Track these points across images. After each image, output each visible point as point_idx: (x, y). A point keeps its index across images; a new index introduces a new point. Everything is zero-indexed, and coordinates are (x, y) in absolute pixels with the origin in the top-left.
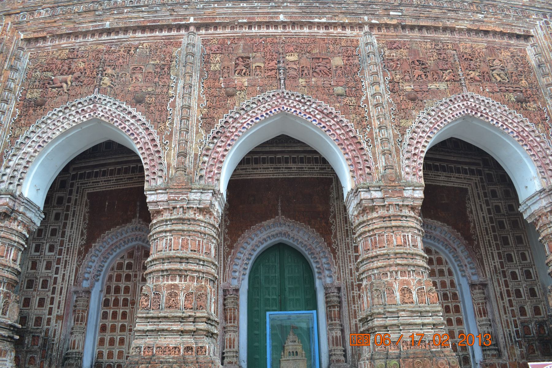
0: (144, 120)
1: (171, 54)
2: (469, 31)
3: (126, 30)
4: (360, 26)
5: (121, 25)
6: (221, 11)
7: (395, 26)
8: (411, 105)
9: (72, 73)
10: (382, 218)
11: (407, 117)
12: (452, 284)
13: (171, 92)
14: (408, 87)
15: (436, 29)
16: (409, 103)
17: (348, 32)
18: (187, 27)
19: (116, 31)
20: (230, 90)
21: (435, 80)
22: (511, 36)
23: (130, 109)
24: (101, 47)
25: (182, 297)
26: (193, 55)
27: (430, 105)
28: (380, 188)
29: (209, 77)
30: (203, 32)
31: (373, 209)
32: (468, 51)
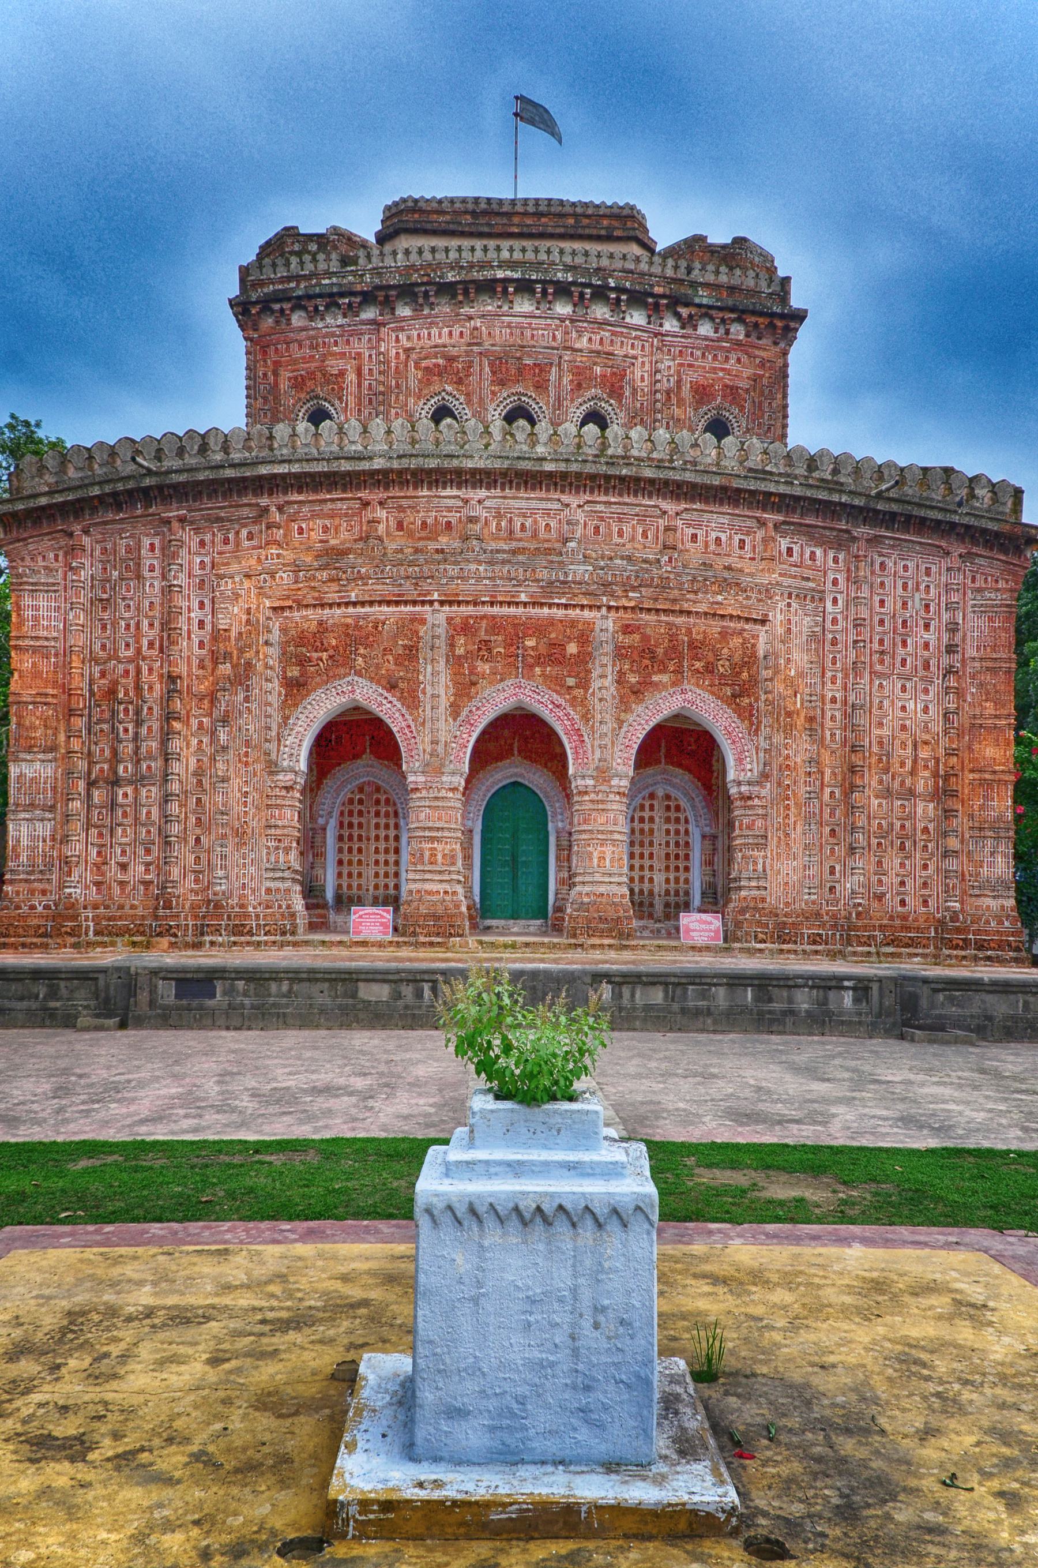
0: (399, 706)
1: (417, 632)
2: (706, 614)
3: (371, 603)
5: (368, 599)
6: (464, 587)
7: (633, 608)
8: (633, 697)
9: (326, 650)
10: (592, 801)
11: (627, 710)
12: (687, 832)
13: (421, 678)
14: (633, 679)
15: (673, 611)
17: (586, 613)
19: (363, 604)
20: (474, 678)
21: (660, 672)
22: (748, 620)
23: (386, 694)
24: (349, 621)
26: (438, 637)
27: (649, 701)
29: (455, 662)
30: (446, 608)
31: (586, 793)
32: (700, 637)
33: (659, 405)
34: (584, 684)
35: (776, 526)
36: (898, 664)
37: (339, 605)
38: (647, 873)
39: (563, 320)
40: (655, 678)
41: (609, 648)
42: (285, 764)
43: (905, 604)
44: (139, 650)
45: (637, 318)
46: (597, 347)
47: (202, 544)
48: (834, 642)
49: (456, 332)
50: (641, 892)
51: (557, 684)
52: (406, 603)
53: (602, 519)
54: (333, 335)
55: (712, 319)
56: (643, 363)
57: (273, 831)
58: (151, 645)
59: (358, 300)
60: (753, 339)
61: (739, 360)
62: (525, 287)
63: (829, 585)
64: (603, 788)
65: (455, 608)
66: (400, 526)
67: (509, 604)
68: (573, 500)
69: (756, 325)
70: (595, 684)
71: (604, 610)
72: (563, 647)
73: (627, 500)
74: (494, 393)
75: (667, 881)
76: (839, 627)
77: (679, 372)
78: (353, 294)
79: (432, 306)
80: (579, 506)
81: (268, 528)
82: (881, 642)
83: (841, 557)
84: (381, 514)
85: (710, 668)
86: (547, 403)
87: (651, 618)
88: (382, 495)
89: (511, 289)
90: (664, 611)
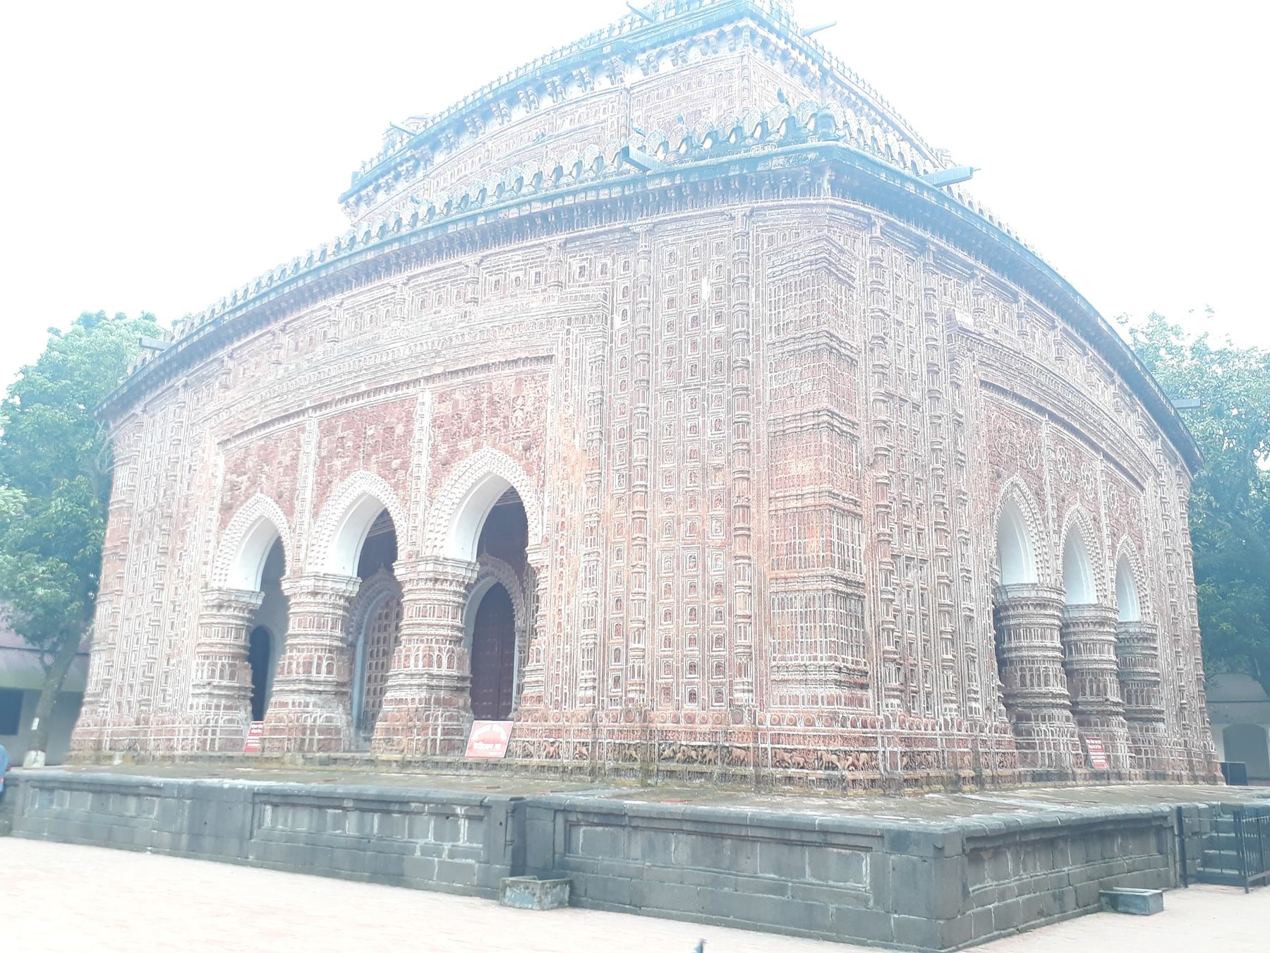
7: (444, 374)
14: (443, 450)
15: (475, 368)
22: (538, 359)
25: (294, 666)
30: (318, 413)
34: (405, 466)
35: (563, 246)
41: (427, 420)
51: (386, 471)
57: (204, 649)
59: (412, 163)
60: (711, 55)
65: (324, 411)
69: (707, 42)
80: (405, 284)
88: (281, 323)
89: (502, 105)
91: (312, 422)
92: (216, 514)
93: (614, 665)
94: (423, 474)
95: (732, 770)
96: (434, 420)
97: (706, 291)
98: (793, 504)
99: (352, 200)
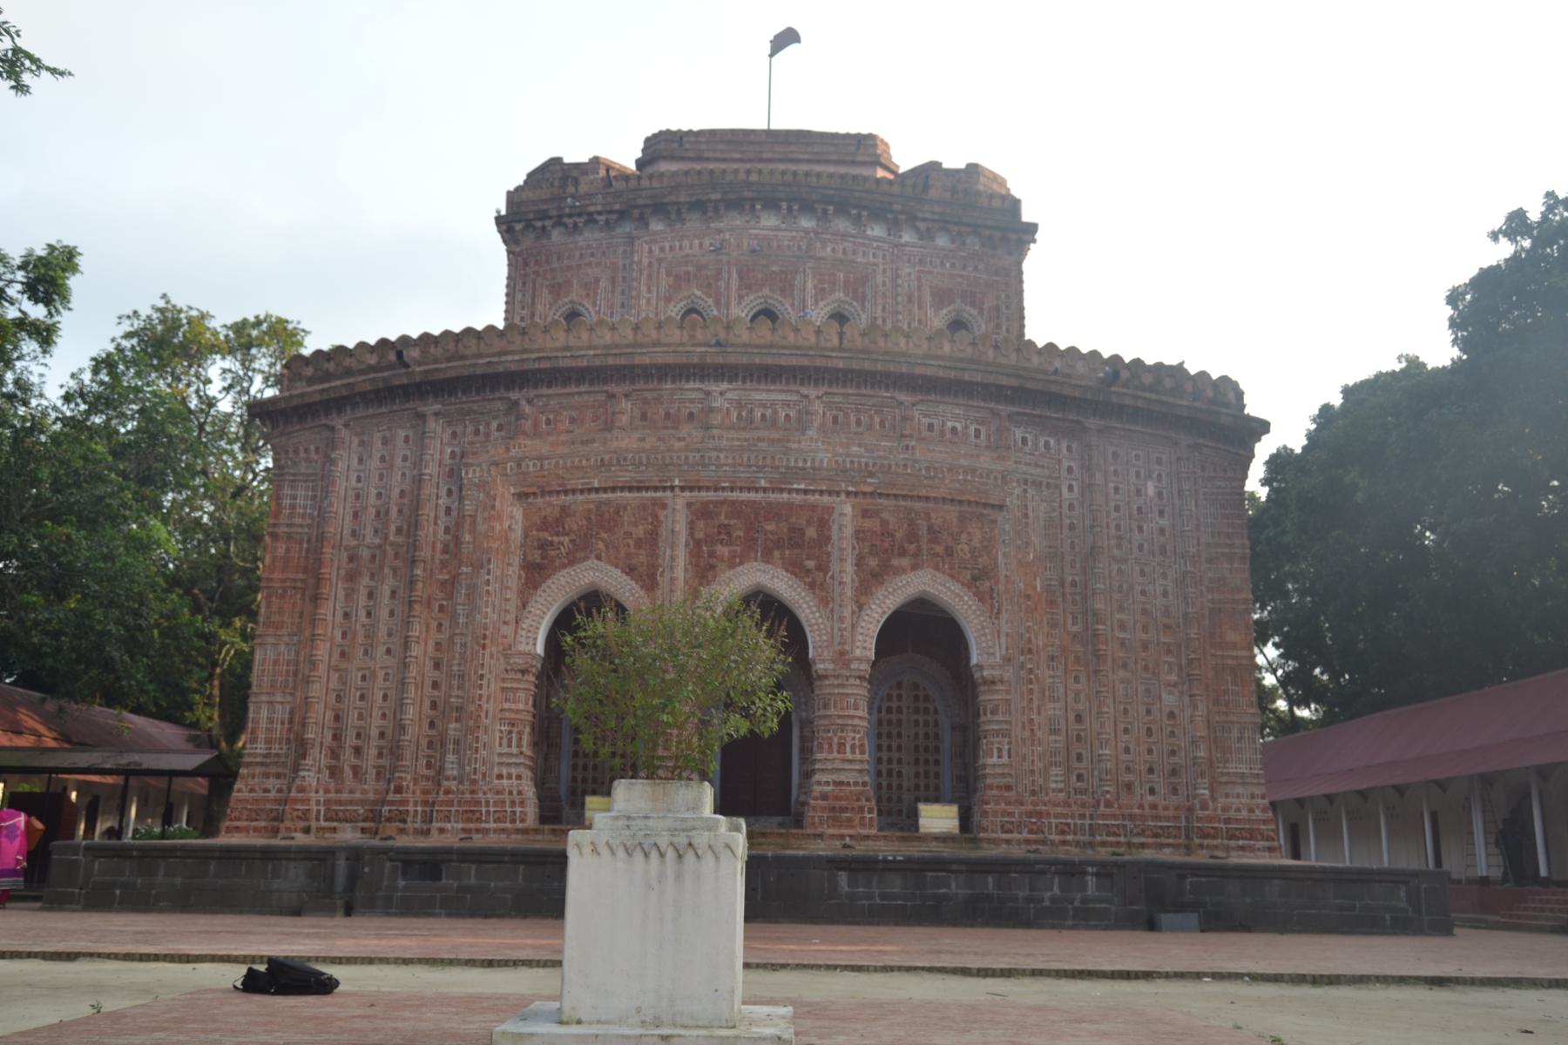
3: (613, 489)
4: (838, 493)
7: (872, 494)
12: (936, 723)
14: (873, 562)
16: (870, 580)
17: (826, 499)
18: (672, 488)
19: (605, 490)
22: (985, 505)
24: (592, 506)
28: (833, 661)
30: (687, 494)
33: (900, 308)
34: (823, 568)
35: (1010, 417)
36: (1135, 551)
37: (582, 491)
38: (895, 766)
39: (806, 232)
40: (895, 562)
41: (849, 531)
42: (522, 647)
43: (1138, 492)
44: (386, 538)
45: (877, 231)
46: (840, 255)
47: (454, 434)
48: (1072, 527)
49: (707, 242)
50: (890, 787)
51: (795, 568)
52: (647, 489)
53: (840, 409)
54: (589, 247)
55: (948, 231)
56: (884, 271)
57: (507, 715)
58: (399, 531)
61: (976, 268)
62: (772, 204)
63: (1064, 473)
64: (844, 672)
65: (695, 493)
66: (644, 417)
67: (749, 490)
68: (812, 392)
70: (835, 567)
71: (843, 496)
72: (802, 531)
73: (863, 391)
74: (741, 297)
75: (917, 775)
76: (1076, 513)
77: (919, 279)
78: (611, 212)
79: (683, 221)
81: (518, 418)
82: (1118, 527)
83: (1074, 446)
84: (625, 405)
85: (949, 552)
86: (792, 305)
87: (892, 502)
88: (626, 388)
90: (904, 497)
91: (680, 501)
92: (514, 570)
93: (1077, 765)
94: (848, 579)
95: (1206, 842)
96: (857, 533)
97: (1151, 491)
98: (1230, 662)
99: (518, 227)
